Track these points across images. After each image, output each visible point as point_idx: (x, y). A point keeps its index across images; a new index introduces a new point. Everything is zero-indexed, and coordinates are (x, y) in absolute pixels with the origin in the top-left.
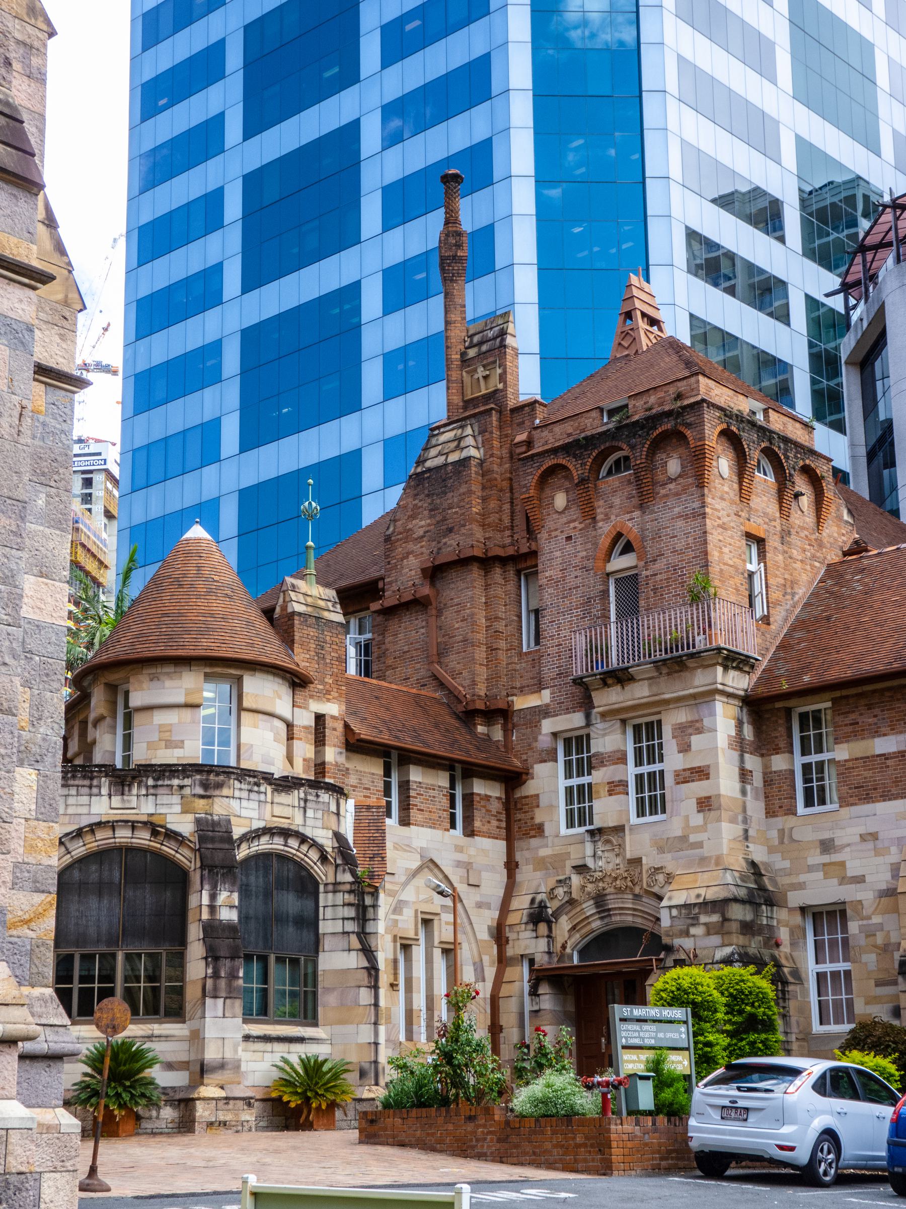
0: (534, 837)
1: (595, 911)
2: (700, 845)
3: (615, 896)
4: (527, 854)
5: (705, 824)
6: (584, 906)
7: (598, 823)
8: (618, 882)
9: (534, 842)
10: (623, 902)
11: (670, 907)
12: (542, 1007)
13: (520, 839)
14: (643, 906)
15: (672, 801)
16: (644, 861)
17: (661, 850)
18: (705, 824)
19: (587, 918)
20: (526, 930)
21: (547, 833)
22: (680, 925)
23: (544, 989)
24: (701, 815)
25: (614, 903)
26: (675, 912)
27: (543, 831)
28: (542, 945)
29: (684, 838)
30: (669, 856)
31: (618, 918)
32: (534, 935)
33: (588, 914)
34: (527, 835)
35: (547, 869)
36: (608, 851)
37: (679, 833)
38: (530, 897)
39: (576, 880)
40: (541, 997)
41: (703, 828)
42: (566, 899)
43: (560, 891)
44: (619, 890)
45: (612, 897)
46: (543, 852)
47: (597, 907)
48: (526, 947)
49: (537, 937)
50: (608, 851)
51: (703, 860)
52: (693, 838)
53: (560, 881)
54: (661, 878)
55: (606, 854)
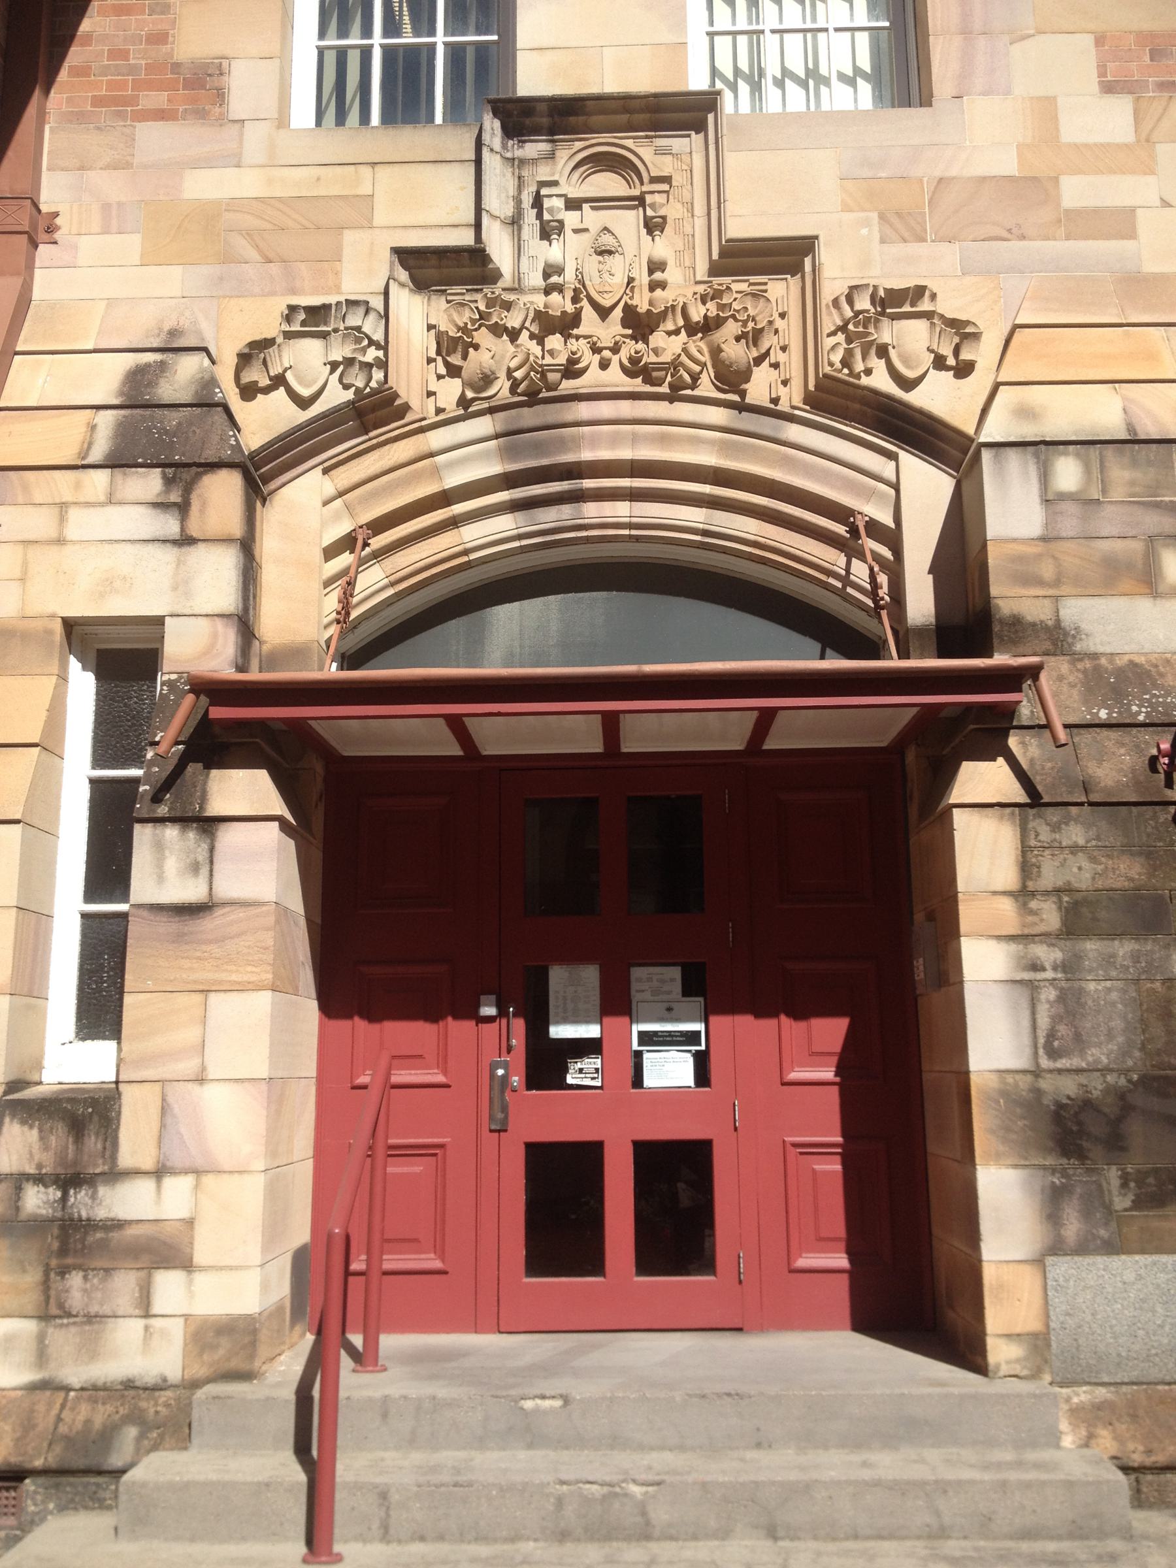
0: (161, 115)
1: (494, 468)
2: (1121, 222)
3: (625, 408)
4: (110, 185)
5: (1146, 141)
6: (437, 439)
7: (534, 78)
8: (658, 339)
9: (154, 139)
10: (663, 440)
11: (1042, 449)
12: (229, 886)
13: (78, 118)
14: (788, 463)
15: (966, 32)
16: (826, 254)
17: (902, 224)
18: (1146, 141)
19: (445, 498)
20: (111, 500)
21: (238, 106)
22: (1117, 531)
23: (243, 790)
24: (1121, 109)
25: (614, 441)
26: (1068, 473)
27: (220, 96)
28: (214, 577)
29: (1031, 189)
30: (949, 256)
31: (621, 510)
32: (170, 525)
33: (453, 480)
34: (121, 105)
35: (228, 258)
36: (600, 202)
37: (1007, 164)
38: (129, 361)
39: (415, 317)
40: (229, 836)
41: (1138, 155)
42: (336, 396)
43: (307, 360)
44: (661, 381)
45: (605, 409)
46: (204, 186)
47: (508, 453)
48: (108, 585)
49: (186, 541)
50: (600, 202)
51: (1135, 284)
52: (1076, 191)
53: (317, 313)
54: (911, 338)
55: (592, 218)
